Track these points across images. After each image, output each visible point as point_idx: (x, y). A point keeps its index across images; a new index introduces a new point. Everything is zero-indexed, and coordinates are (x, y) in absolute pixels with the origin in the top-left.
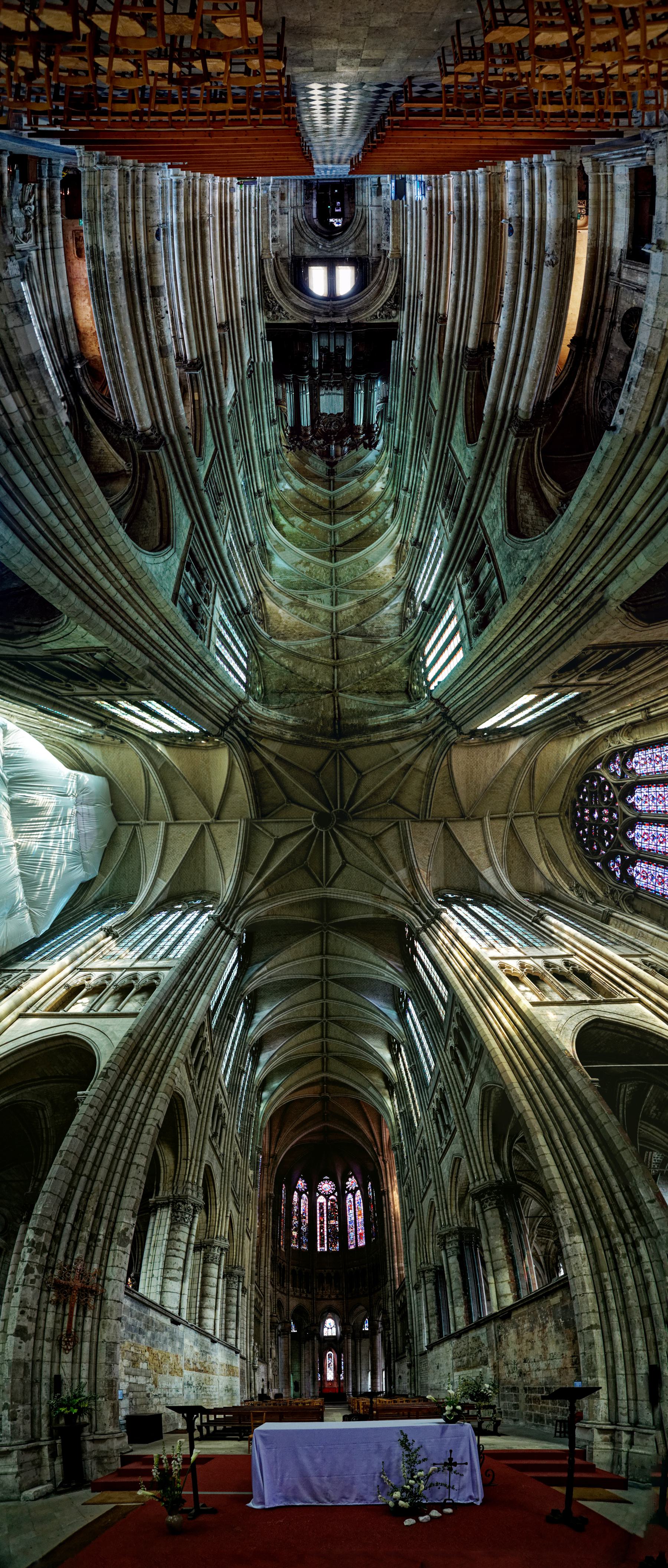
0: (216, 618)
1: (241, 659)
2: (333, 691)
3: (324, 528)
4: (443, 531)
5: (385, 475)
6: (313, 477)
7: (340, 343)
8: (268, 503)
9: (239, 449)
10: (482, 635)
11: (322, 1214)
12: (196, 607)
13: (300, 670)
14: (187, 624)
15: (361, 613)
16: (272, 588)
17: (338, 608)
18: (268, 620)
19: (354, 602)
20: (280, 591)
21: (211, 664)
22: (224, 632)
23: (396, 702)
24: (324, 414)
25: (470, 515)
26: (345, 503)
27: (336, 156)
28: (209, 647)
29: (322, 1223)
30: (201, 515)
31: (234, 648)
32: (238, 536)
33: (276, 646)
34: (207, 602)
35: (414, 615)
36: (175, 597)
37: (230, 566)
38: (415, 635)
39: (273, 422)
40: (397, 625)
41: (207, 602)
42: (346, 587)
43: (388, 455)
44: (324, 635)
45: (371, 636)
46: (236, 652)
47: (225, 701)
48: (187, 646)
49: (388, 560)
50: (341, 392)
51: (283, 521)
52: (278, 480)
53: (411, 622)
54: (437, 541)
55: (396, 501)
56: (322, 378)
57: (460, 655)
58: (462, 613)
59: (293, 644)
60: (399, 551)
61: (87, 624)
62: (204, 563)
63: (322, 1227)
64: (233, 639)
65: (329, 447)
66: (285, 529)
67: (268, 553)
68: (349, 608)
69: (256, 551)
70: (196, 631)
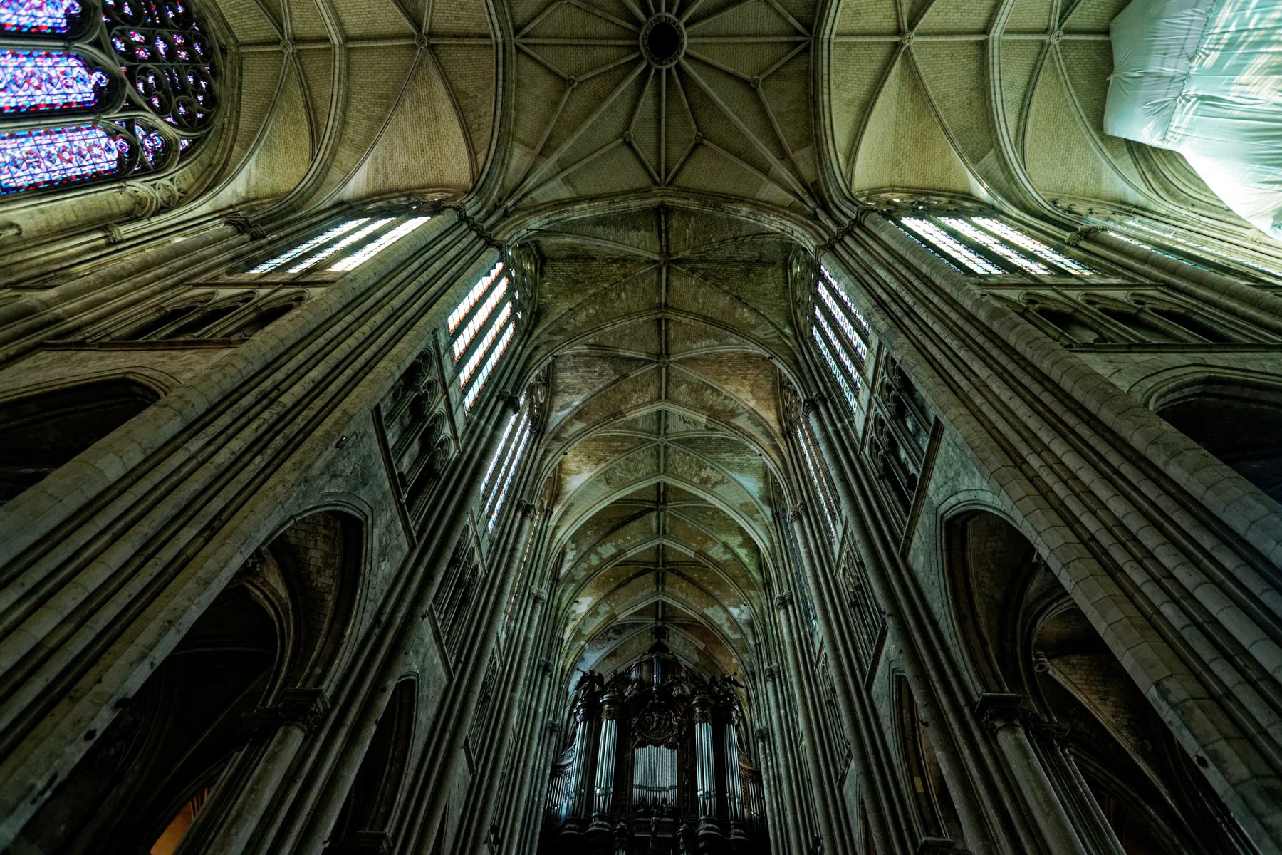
0: (864, 395)
1: (825, 324)
2: (668, 263)
3: (675, 540)
4: (479, 528)
6: (691, 626)
8: (767, 585)
10: (415, 354)
12: (900, 414)
13: (723, 302)
14: (918, 387)
15: (619, 396)
16: (765, 441)
17: (657, 407)
18: (773, 389)
19: (631, 416)
20: (750, 436)
21: (877, 317)
22: (852, 370)
23: (561, 241)
24: (669, 746)
26: (642, 579)
28: (880, 345)
30: (890, 571)
31: (835, 342)
32: (821, 530)
33: (762, 343)
34: (879, 422)
35: (532, 391)
36: (937, 431)
37: (836, 481)
38: (530, 357)
39: (764, 735)
40: (561, 375)
41: (879, 422)
42: (643, 442)
43: (562, 662)
44: (680, 362)
45: (603, 358)
46: (832, 336)
47: (859, 251)
48: (921, 349)
50: (638, 793)
51: (743, 553)
52: (751, 624)
53: (538, 378)
54: (491, 511)
55: (555, 580)
56: (674, 826)
57: (453, 320)
58: (451, 390)
59: (733, 346)
60: (556, 496)
61: (1108, 393)
62: (883, 488)
64: (836, 357)
65: (663, 677)
66: (740, 539)
67: (768, 501)
68: (638, 406)
69: (789, 505)
70: (901, 373)
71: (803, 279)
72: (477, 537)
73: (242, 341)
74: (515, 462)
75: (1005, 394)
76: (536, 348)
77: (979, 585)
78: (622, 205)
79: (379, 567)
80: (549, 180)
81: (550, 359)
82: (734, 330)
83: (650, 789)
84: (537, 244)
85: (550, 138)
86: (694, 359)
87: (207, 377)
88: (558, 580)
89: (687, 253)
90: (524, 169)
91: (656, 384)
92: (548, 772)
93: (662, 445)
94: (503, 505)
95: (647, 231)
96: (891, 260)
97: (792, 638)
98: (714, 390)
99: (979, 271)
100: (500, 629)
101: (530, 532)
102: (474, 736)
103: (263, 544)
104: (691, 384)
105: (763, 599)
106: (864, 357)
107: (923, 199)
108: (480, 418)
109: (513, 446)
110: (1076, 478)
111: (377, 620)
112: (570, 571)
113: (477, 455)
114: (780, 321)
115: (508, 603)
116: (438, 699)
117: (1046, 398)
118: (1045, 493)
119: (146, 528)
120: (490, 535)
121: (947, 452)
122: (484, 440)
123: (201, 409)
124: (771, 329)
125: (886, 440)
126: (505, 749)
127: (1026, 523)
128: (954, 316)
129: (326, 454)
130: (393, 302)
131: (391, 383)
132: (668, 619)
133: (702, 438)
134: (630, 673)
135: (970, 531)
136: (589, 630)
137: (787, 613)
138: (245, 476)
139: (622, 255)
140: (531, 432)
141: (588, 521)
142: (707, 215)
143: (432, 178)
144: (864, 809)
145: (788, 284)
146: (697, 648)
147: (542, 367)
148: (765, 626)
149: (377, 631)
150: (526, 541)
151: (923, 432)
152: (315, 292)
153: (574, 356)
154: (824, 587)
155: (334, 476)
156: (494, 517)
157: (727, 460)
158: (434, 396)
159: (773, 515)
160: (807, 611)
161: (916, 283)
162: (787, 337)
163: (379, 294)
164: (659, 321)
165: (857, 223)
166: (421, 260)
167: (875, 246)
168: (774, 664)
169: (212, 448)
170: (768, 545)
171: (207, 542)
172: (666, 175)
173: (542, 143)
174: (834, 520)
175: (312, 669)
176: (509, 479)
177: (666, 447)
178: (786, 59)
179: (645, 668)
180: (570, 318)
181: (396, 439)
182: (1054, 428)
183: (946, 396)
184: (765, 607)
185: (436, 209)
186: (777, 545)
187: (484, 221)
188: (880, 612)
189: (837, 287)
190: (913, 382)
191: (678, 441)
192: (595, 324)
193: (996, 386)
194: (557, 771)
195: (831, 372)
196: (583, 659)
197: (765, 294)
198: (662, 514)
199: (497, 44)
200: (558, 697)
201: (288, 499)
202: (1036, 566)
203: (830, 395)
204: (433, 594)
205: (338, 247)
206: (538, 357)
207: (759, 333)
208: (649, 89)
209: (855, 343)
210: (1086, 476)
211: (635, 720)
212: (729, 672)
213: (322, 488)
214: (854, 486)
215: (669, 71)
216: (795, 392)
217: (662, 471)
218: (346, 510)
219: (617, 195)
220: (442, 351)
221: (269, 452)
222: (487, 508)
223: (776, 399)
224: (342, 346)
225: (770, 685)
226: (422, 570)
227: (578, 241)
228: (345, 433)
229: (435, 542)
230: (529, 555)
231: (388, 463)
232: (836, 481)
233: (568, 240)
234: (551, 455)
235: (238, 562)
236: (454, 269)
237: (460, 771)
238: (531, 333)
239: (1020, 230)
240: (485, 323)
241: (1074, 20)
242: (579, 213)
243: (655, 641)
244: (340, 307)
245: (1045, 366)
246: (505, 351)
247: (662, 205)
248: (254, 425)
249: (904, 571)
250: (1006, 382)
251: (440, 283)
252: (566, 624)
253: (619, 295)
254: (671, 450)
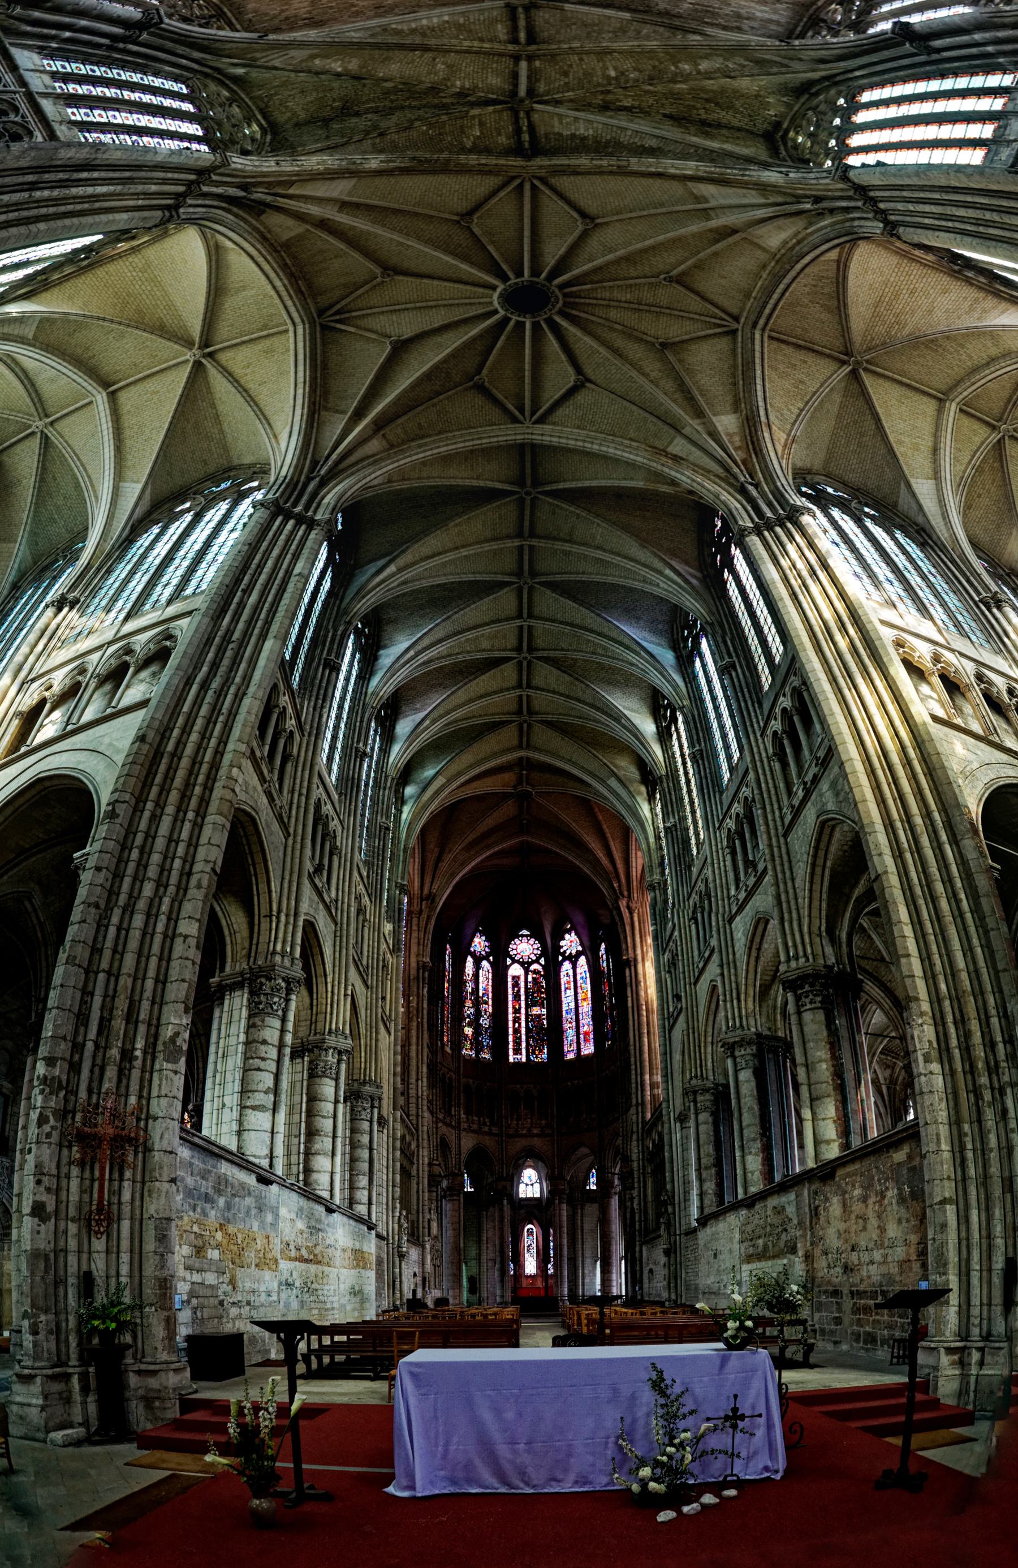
11: (517, 997)
29: (517, 1011)
63: (517, 1020)
78: (605, 163)
89: (475, 112)
95: (560, 135)
139: (609, 113)
142: (442, 151)
178: (348, 300)
199: (763, 330)
208: (550, 261)
215: (519, 274)
219: (611, 173)
241: (35, 443)
242: (690, 167)
247: (528, 158)
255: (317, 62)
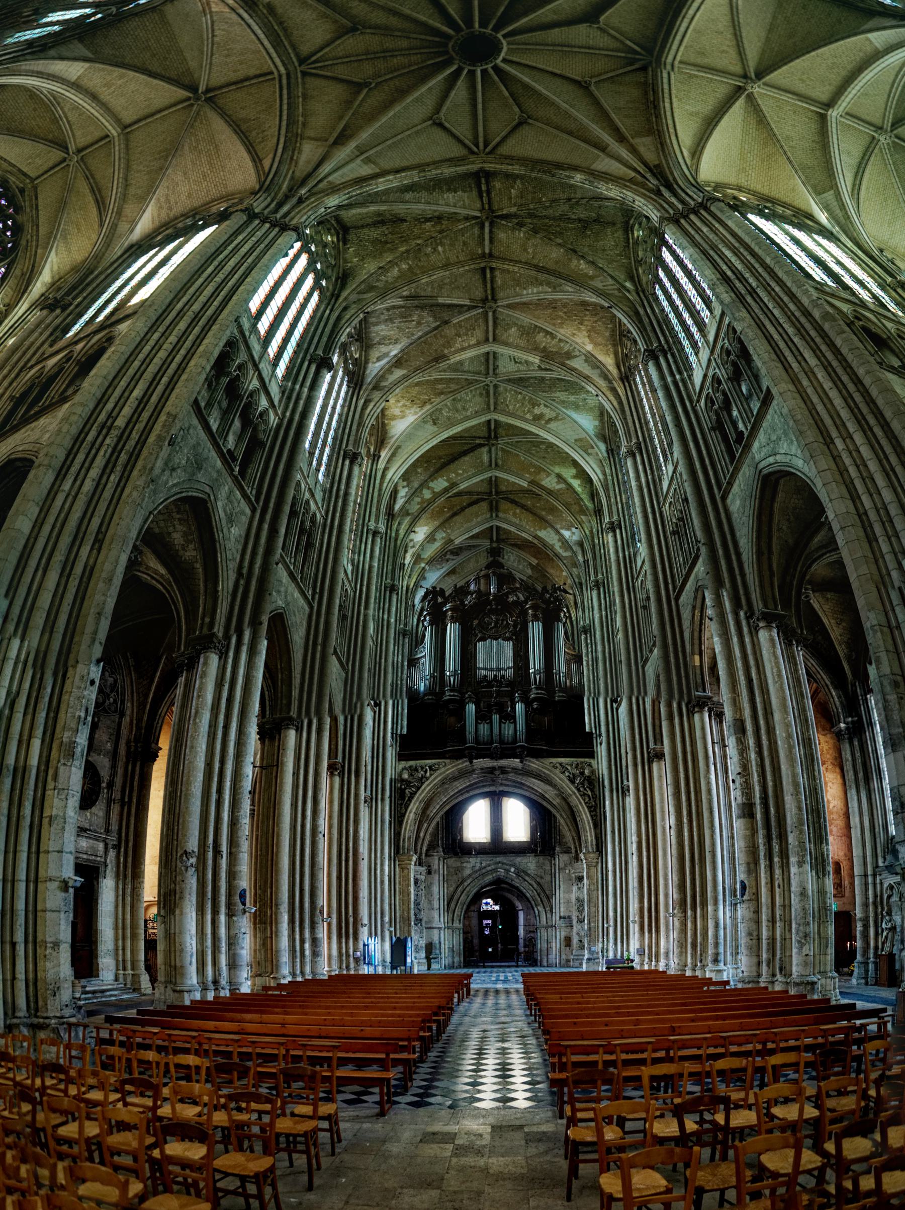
0: (705, 354)
1: (668, 284)
3: (509, 471)
4: (311, 481)
5: (410, 552)
6: (524, 546)
7: (484, 728)
8: (598, 512)
9: (641, 596)
10: (222, 344)
12: (736, 377)
14: (755, 357)
16: (602, 383)
17: (485, 349)
18: (613, 335)
20: (587, 378)
21: (721, 289)
22: (694, 329)
24: (506, 639)
25: (270, 511)
26: (475, 508)
27: (490, 1002)
28: (723, 314)
30: (710, 509)
31: (678, 302)
32: (652, 467)
34: (716, 380)
35: (344, 348)
37: (671, 426)
38: (339, 318)
39: (587, 630)
41: (716, 380)
42: (470, 383)
44: (509, 306)
45: (422, 307)
46: (675, 296)
47: (705, 229)
48: (760, 326)
49: (399, 427)
50: (481, 673)
51: (576, 484)
52: (581, 544)
53: (350, 335)
55: (391, 515)
57: (254, 305)
58: (262, 366)
59: (568, 293)
60: (381, 442)
62: (714, 439)
64: (679, 316)
65: (500, 587)
66: (573, 471)
67: (604, 438)
68: (463, 349)
69: (624, 442)
70: (740, 341)
71: (646, 242)
72: (310, 489)
73: (76, 392)
74: (336, 417)
75: (827, 385)
76: (345, 309)
77: (778, 530)
78: (434, 172)
79: (230, 532)
80: (347, 163)
81: (361, 316)
82: (569, 279)
83: (491, 670)
84: (338, 219)
85: (344, 129)
86: (525, 303)
87: (59, 431)
88: (393, 516)
89: (514, 210)
90: (316, 159)
91: (483, 327)
92: (406, 663)
93: (491, 385)
94: (330, 457)
95: (464, 191)
96: (737, 245)
97: (618, 557)
98: (547, 333)
99: (818, 278)
100: (345, 562)
101: (359, 477)
102: (340, 645)
103: (136, 540)
104: (523, 327)
105: (594, 523)
106: (707, 321)
107: (769, 205)
108: (294, 383)
109: (332, 402)
110: (866, 466)
111: (240, 574)
112: (403, 506)
113: (297, 417)
114: (621, 276)
115: (349, 540)
116: (305, 623)
117: (858, 397)
118: (842, 471)
119: (59, 557)
120: (322, 486)
121: (773, 419)
122: (302, 402)
123: (62, 455)
124: (611, 281)
125: (722, 397)
126: (368, 652)
127: (824, 490)
128: (792, 306)
129: (161, 454)
130: (194, 307)
131: (204, 376)
132: (503, 540)
133: (535, 378)
134: (469, 586)
135: (780, 487)
136: (428, 554)
137: (615, 536)
138: (107, 494)
139: (436, 214)
140: (348, 386)
141: (417, 460)
142: (536, 178)
143: (214, 193)
144: (659, 680)
145: (629, 245)
146: (530, 564)
147: (353, 324)
148: (594, 546)
149: (242, 582)
150: (358, 485)
151: (755, 397)
152: (123, 327)
153: (388, 309)
154: (650, 516)
155: (173, 469)
156: (323, 469)
157: (562, 398)
158: (245, 375)
159: (607, 451)
160: (633, 535)
161: (760, 270)
162: (628, 291)
163: (179, 306)
164: (483, 270)
165: (703, 206)
166: (216, 263)
167: (721, 229)
168: (600, 576)
169: (78, 483)
170: (601, 477)
171: (99, 552)
172: (486, 146)
173: (335, 135)
174: (666, 460)
175: (203, 619)
176: (332, 433)
177: (496, 386)
178: (621, 71)
179: (482, 581)
180: (380, 275)
181: (218, 422)
182: (859, 422)
183: (779, 371)
184: (595, 530)
185: (222, 217)
186: (609, 478)
187: (276, 211)
188: (697, 541)
189: (682, 255)
190: (751, 352)
191: (509, 380)
192: (409, 278)
193: (821, 374)
194: (413, 662)
195: (673, 329)
196: (425, 578)
197: (604, 250)
198: (493, 449)
200: (406, 609)
201: (143, 500)
202: (823, 524)
203: (670, 349)
204: (280, 544)
205: (133, 283)
206: (347, 317)
207: (597, 283)
208: (461, 83)
209: (698, 307)
210: (873, 466)
211: (476, 622)
212: (559, 582)
213: (166, 483)
214: (688, 433)
215: (484, 72)
216: (635, 341)
217: (492, 408)
218: (190, 494)
219: (428, 165)
220: (247, 334)
221: (119, 468)
222: (315, 462)
223: (614, 345)
224: (155, 361)
225: (595, 593)
226: (266, 526)
227: (384, 208)
228: (173, 431)
229: (273, 501)
230: (362, 497)
231: (216, 445)
232: (671, 426)
233: (372, 208)
234: (372, 405)
235: (124, 558)
236: (250, 260)
237: (335, 670)
238: (338, 296)
239: (852, 259)
240: (287, 298)
242: (381, 185)
243: (491, 559)
244: (146, 329)
245: (861, 372)
246: (312, 318)
247: (481, 170)
248: (102, 452)
249: (722, 511)
250: (829, 375)
251: (237, 276)
252: (406, 552)
253: (435, 250)
254: (501, 389)
255: (591, 273)
